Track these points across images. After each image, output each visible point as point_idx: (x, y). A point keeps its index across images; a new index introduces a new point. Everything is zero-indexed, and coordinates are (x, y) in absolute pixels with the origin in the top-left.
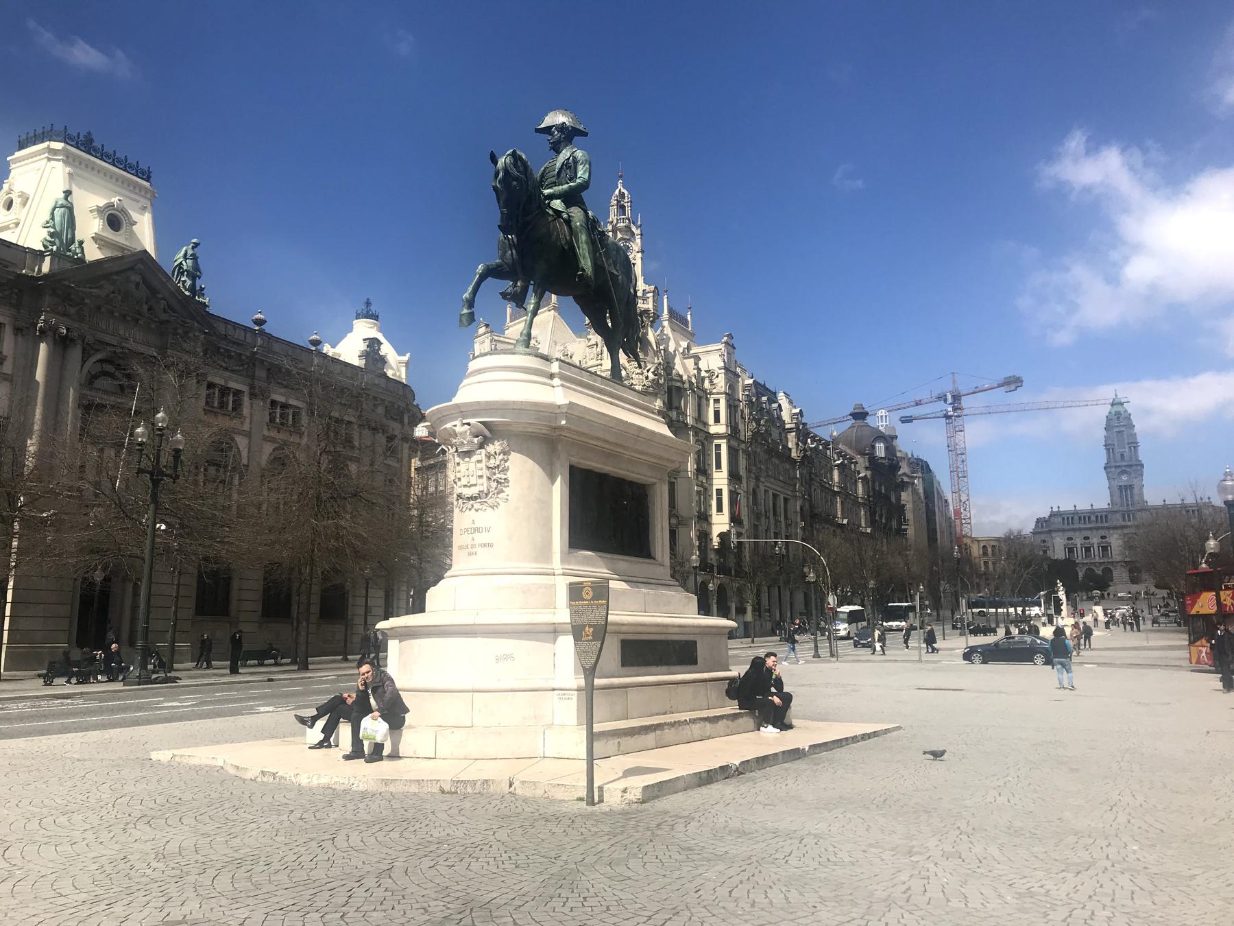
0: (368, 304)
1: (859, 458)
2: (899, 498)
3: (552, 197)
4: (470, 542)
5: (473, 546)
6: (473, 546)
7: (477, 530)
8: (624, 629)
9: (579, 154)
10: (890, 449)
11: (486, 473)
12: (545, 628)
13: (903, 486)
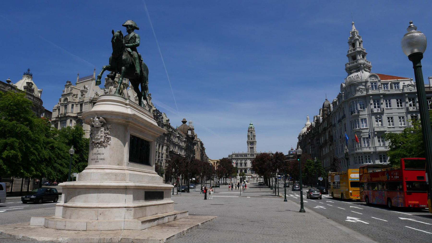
0: (29, 70)
2: (193, 147)
3: (128, 47)
4: (96, 158)
5: (97, 159)
6: (97, 159)
8: (146, 188)
9: (137, 35)
10: (192, 133)
12: (123, 187)
13: (195, 144)
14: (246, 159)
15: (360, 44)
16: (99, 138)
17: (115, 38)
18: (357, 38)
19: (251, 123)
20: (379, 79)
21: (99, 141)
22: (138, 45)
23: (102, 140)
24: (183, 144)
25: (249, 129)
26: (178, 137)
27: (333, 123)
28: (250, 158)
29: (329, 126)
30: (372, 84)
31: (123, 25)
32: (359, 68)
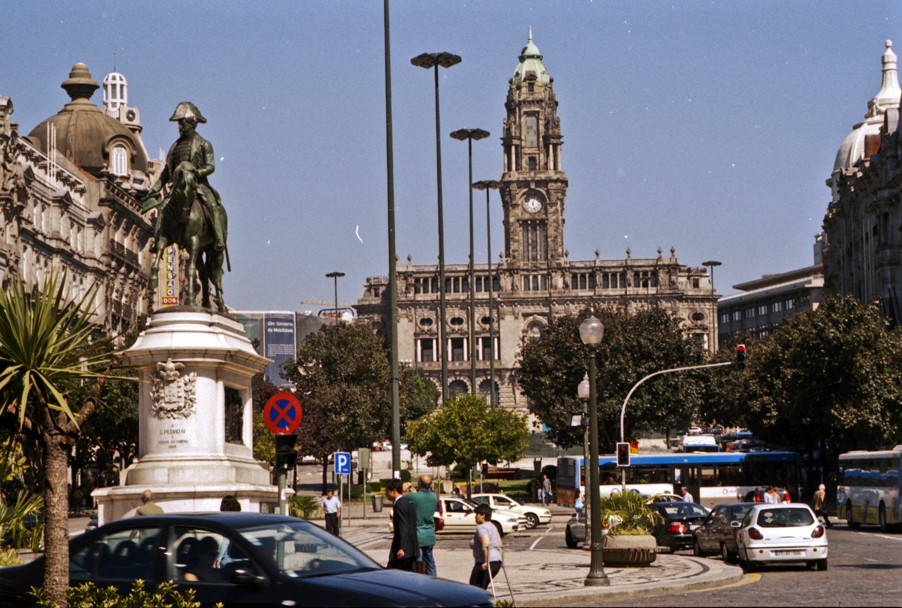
1: (85, 181)
5: (173, 442)
7: (177, 432)
11: (183, 394)
14: (493, 304)
16: (174, 399)
17: (187, 188)
19: (533, 49)
21: (175, 406)
22: (211, 172)
23: (182, 404)
24: (90, 244)
25: (515, 85)
26: (64, 203)
28: (523, 302)
31: (171, 120)
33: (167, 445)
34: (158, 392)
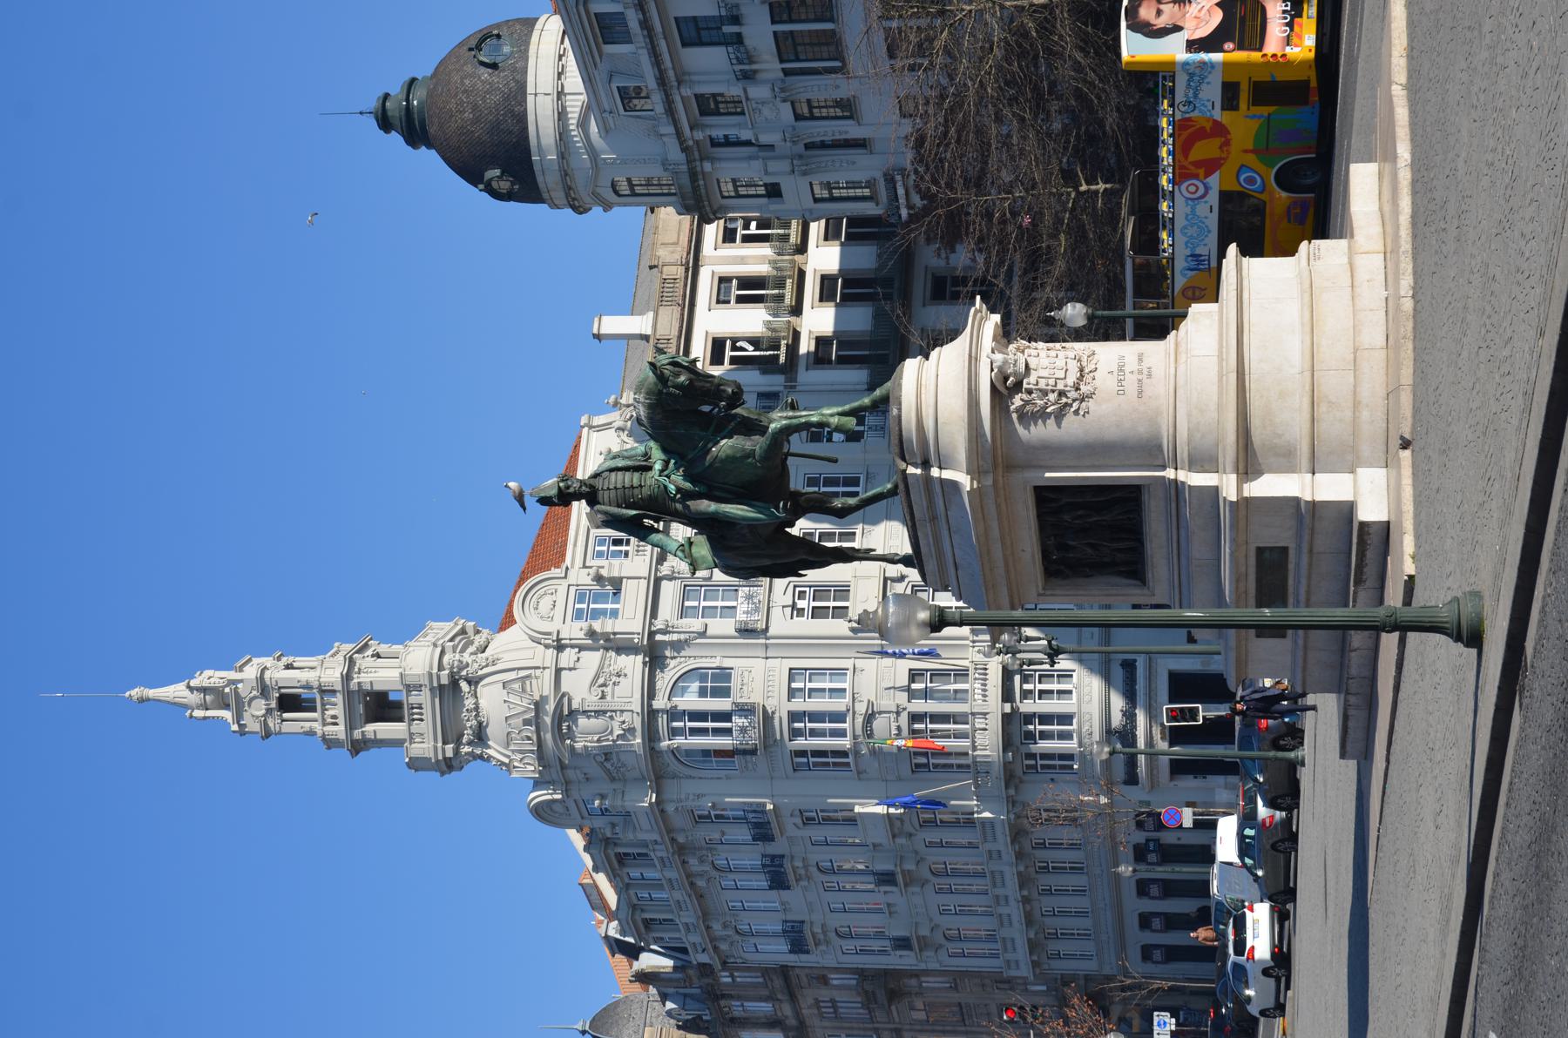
4: (1135, 377)
5: (1140, 372)
6: (1140, 372)
7: (1121, 369)
11: (1053, 353)
15: (289, 667)
16: (1060, 363)
18: (251, 672)
20: (555, 572)
27: (776, 951)
29: (787, 1010)
30: (578, 615)
32: (454, 683)
33: (1145, 381)
34: (1045, 393)
